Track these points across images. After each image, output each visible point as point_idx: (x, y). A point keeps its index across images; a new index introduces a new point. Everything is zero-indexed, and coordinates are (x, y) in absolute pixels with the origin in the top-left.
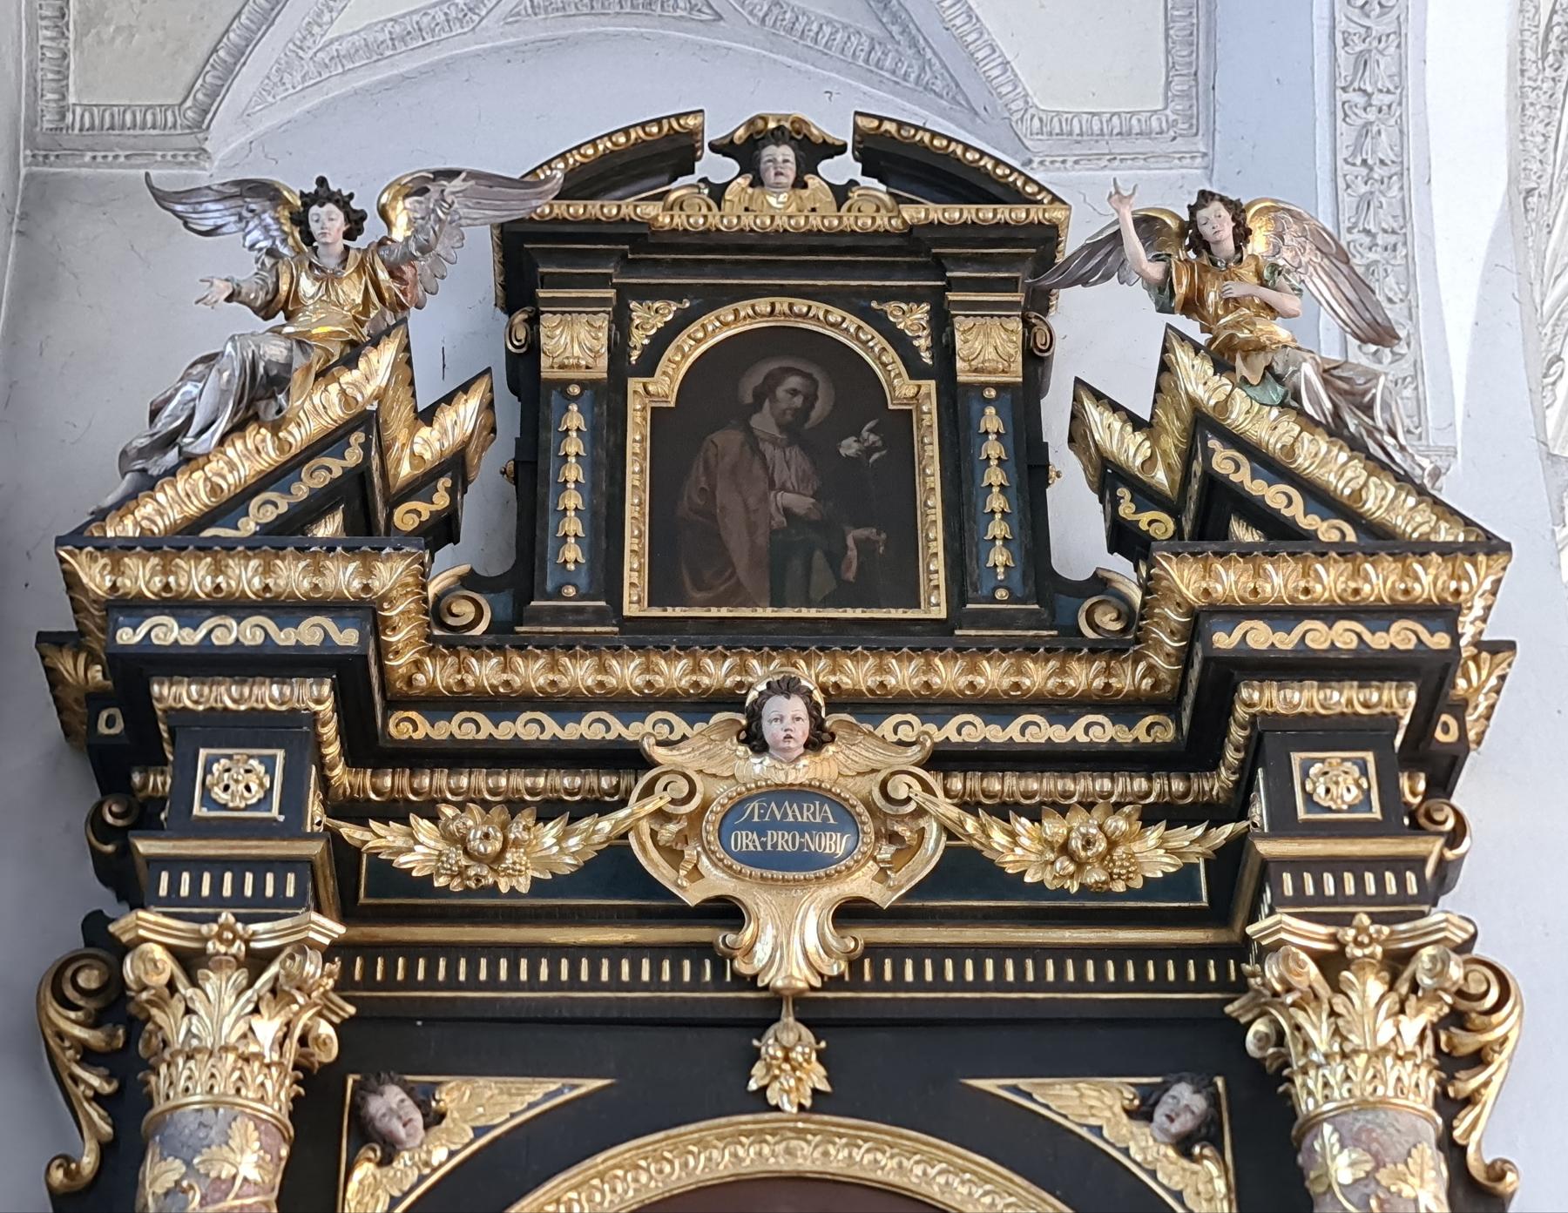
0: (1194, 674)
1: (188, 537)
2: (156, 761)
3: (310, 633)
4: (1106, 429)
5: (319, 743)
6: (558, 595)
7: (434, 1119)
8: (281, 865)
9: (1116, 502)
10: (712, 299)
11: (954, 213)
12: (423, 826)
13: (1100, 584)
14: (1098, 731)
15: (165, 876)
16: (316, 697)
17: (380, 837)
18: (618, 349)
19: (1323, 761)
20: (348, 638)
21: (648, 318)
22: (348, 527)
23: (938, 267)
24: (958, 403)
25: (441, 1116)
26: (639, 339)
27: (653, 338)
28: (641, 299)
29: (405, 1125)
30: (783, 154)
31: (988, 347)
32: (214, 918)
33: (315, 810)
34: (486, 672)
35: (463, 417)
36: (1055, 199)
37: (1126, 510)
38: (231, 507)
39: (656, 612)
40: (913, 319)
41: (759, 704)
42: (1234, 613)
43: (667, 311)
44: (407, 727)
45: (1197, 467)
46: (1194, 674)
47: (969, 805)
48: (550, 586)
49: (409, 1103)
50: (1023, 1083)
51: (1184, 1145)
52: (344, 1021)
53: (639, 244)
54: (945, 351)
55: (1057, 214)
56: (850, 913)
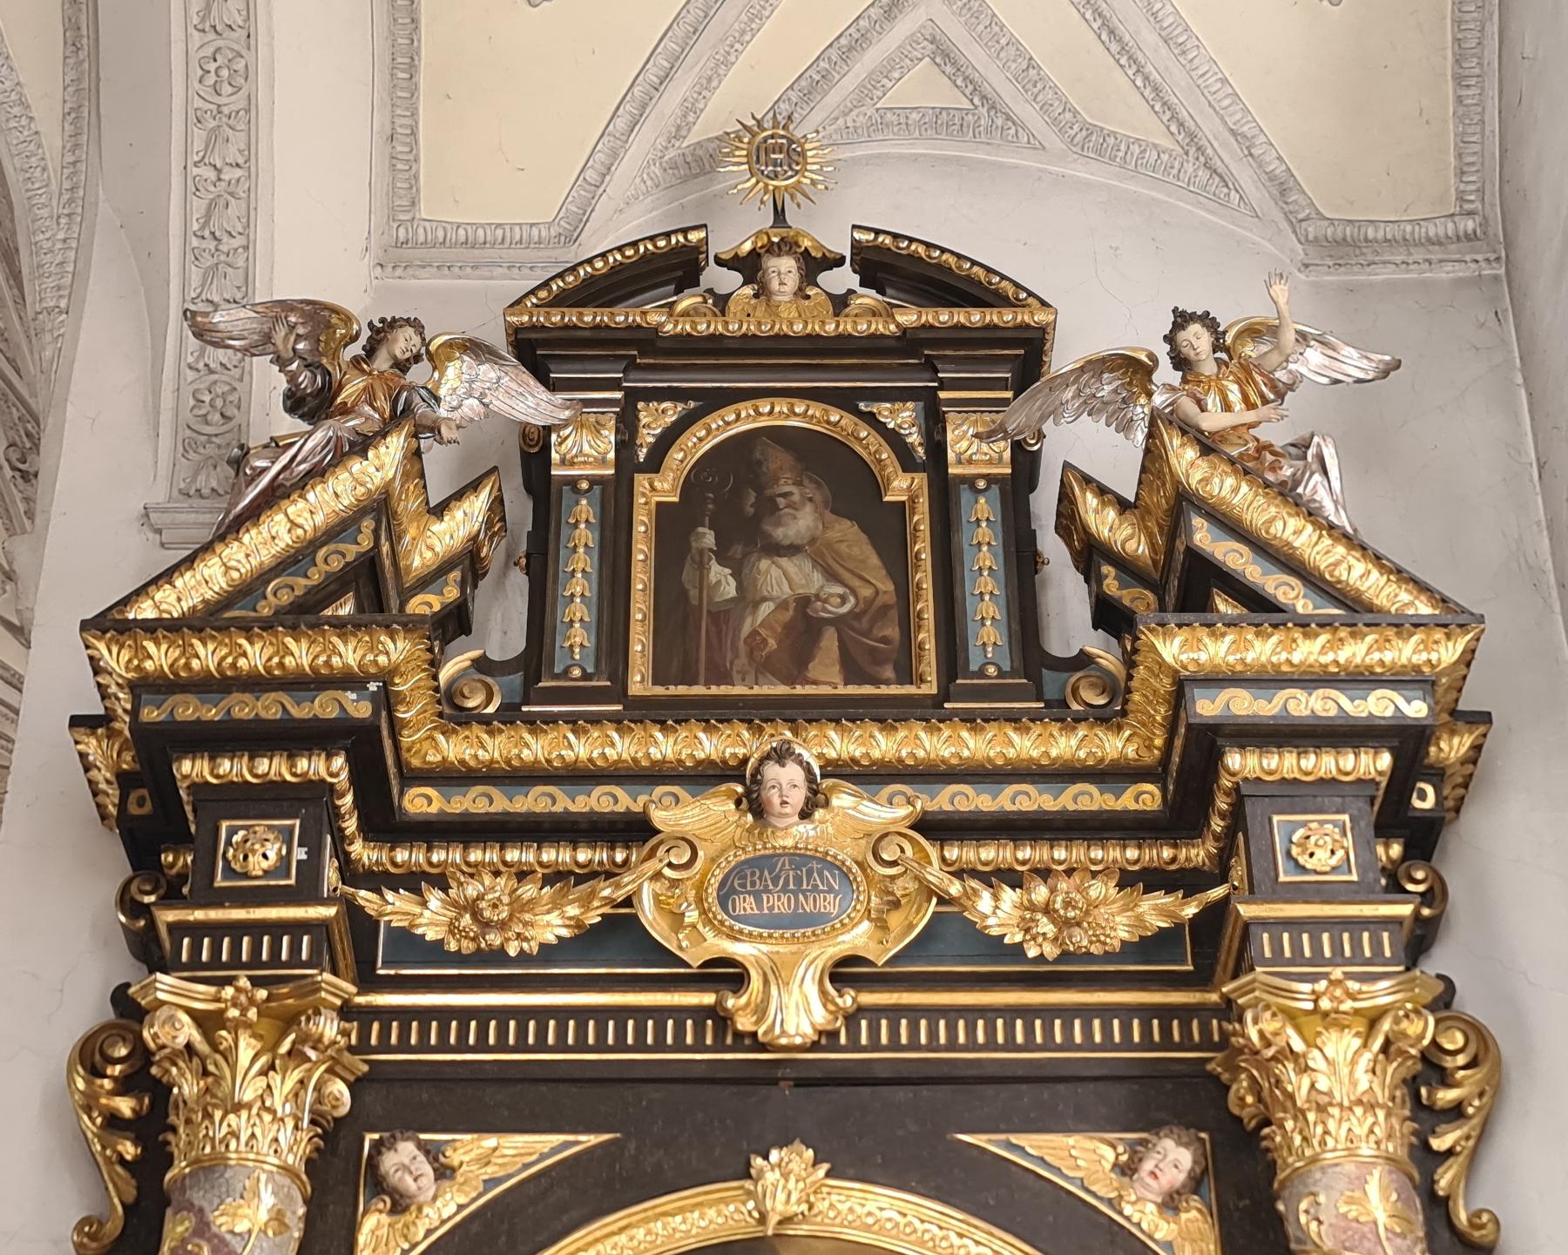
0: (1178, 742)
1: (208, 620)
2: (182, 839)
3: (324, 707)
5: (336, 814)
6: (565, 674)
7: (444, 1173)
8: (296, 928)
9: (1100, 579)
11: (944, 317)
12: (435, 898)
13: (1083, 660)
16: (334, 768)
17: (394, 907)
18: (625, 446)
19: (1304, 824)
20: (359, 708)
22: (360, 608)
23: (931, 367)
24: (945, 494)
26: (647, 437)
28: (647, 400)
29: (415, 1180)
32: (230, 981)
33: (331, 874)
34: (494, 748)
36: (1044, 304)
38: (248, 590)
39: (659, 690)
40: (903, 418)
41: (757, 770)
42: (1217, 680)
43: (671, 412)
44: (419, 802)
45: (1180, 546)
46: (1178, 742)
49: (421, 1158)
50: (1015, 1139)
52: (358, 1080)
53: (646, 341)
54: (937, 449)
55: (1041, 317)
56: (845, 972)
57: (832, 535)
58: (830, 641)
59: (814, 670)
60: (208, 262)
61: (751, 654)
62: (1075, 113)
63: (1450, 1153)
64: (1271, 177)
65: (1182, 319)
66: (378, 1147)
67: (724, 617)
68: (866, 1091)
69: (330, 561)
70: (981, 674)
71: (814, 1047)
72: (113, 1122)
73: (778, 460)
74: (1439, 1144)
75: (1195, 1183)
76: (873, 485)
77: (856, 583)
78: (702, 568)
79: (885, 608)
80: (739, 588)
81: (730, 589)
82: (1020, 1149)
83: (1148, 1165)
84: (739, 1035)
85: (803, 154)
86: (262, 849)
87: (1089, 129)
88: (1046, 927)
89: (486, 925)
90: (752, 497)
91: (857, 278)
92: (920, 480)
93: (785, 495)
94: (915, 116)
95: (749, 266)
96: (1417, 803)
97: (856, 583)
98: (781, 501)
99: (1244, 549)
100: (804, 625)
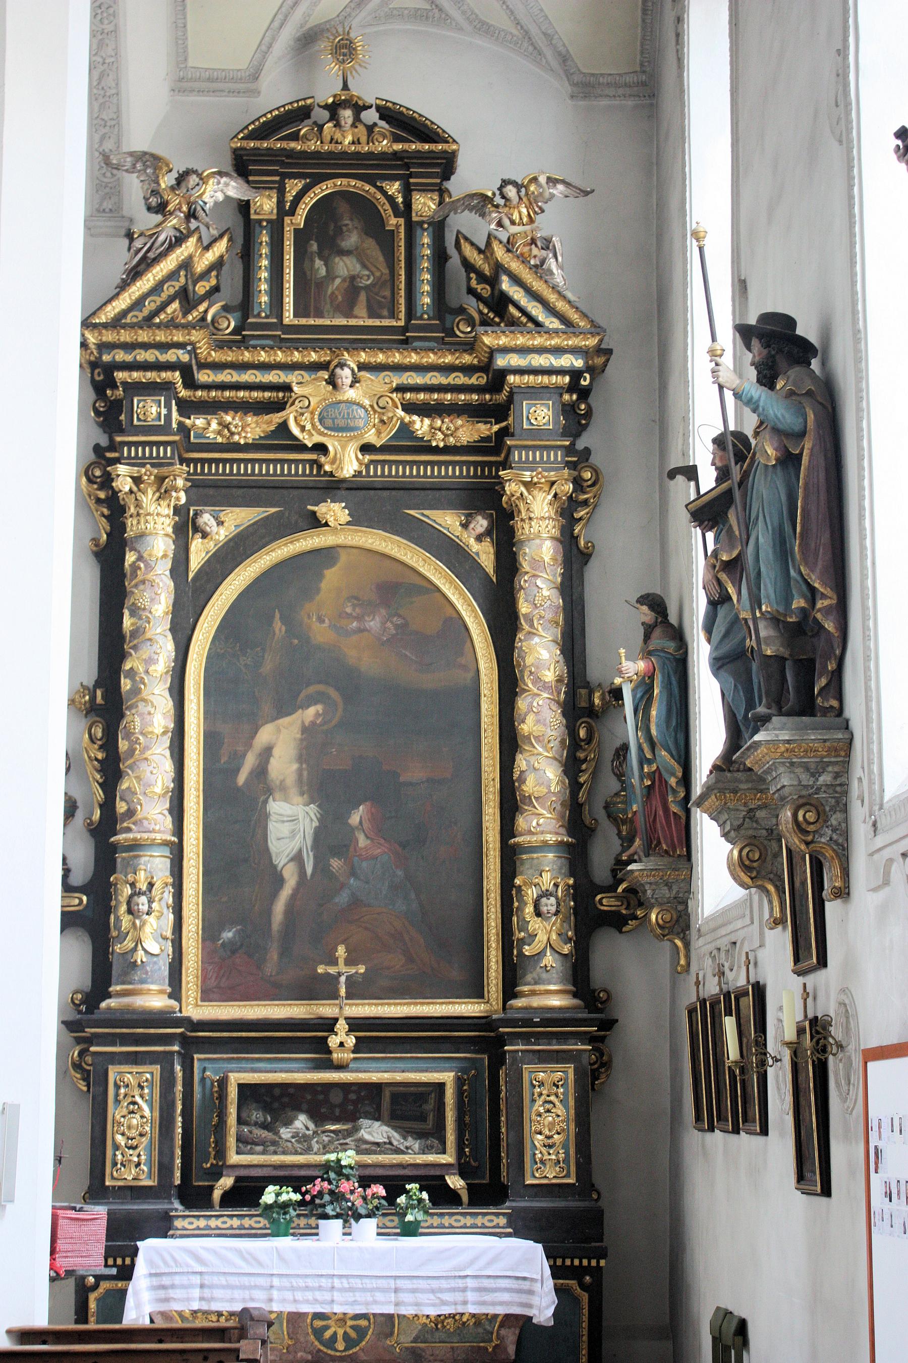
3: (171, 356)
4: (468, 250)
6: (259, 315)
8: (165, 444)
10: (318, 179)
14: (460, 379)
15: (126, 448)
18: (281, 202)
20: (185, 358)
21: (293, 187)
23: (407, 166)
24: (411, 227)
25: (223, 523)
26: (289, 197)
27: (295, 197)
30: (347, 115)
31: (425, 204)
35: (221, 247)
36: (454, 141)
37: (474, 283)
40: (394, 188)
42: (505, 350)
47: (409, 408)
48: (255, 313)
49: (212, 519)
50: (426, 512)
51: (479, 538)
54: (408, 204)
55: (454, 147)
56: (366, 448)
57: (365, 245)
58: (363, 297)
59: (356, 311)
60: (101, 100)
61: (331, 303)
62: (477, 16)
63: (580, 519)
64: (560, 53)
65: (505, 183)
66: (196, 514)
67: (321, 285)
68: (372, 492)
69: (169, 290)
70: (421, 318)
71: (354, 476)
72: (99, 501)
73: (343, 207)
74: (576, 515)
75: (488, 532)
76: (382, 222)
77: (374, 269)
78: (313, 261)
79: (385, 282)
80: (327, 271)
81: (323, 272)
82: (428, 517)
83: (472, 526)
84: (326, 472)
85: (355, 49)
86: (150, 409)
87: (483, 23)
88: (440, 436)
89: (232, 434)
90: (332, 227)
91: (377, 115)
92: (402, 221)
93: (347, 225)
94: (406, 12)
95: (333, 109)
96: (583, 383)
97: (374, 269)
98: (344, 228)
99: (521, 290)
100: (352, 289)
